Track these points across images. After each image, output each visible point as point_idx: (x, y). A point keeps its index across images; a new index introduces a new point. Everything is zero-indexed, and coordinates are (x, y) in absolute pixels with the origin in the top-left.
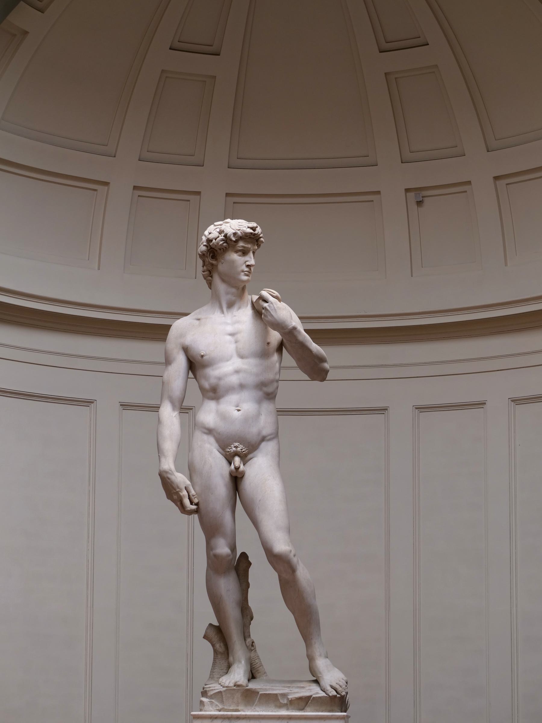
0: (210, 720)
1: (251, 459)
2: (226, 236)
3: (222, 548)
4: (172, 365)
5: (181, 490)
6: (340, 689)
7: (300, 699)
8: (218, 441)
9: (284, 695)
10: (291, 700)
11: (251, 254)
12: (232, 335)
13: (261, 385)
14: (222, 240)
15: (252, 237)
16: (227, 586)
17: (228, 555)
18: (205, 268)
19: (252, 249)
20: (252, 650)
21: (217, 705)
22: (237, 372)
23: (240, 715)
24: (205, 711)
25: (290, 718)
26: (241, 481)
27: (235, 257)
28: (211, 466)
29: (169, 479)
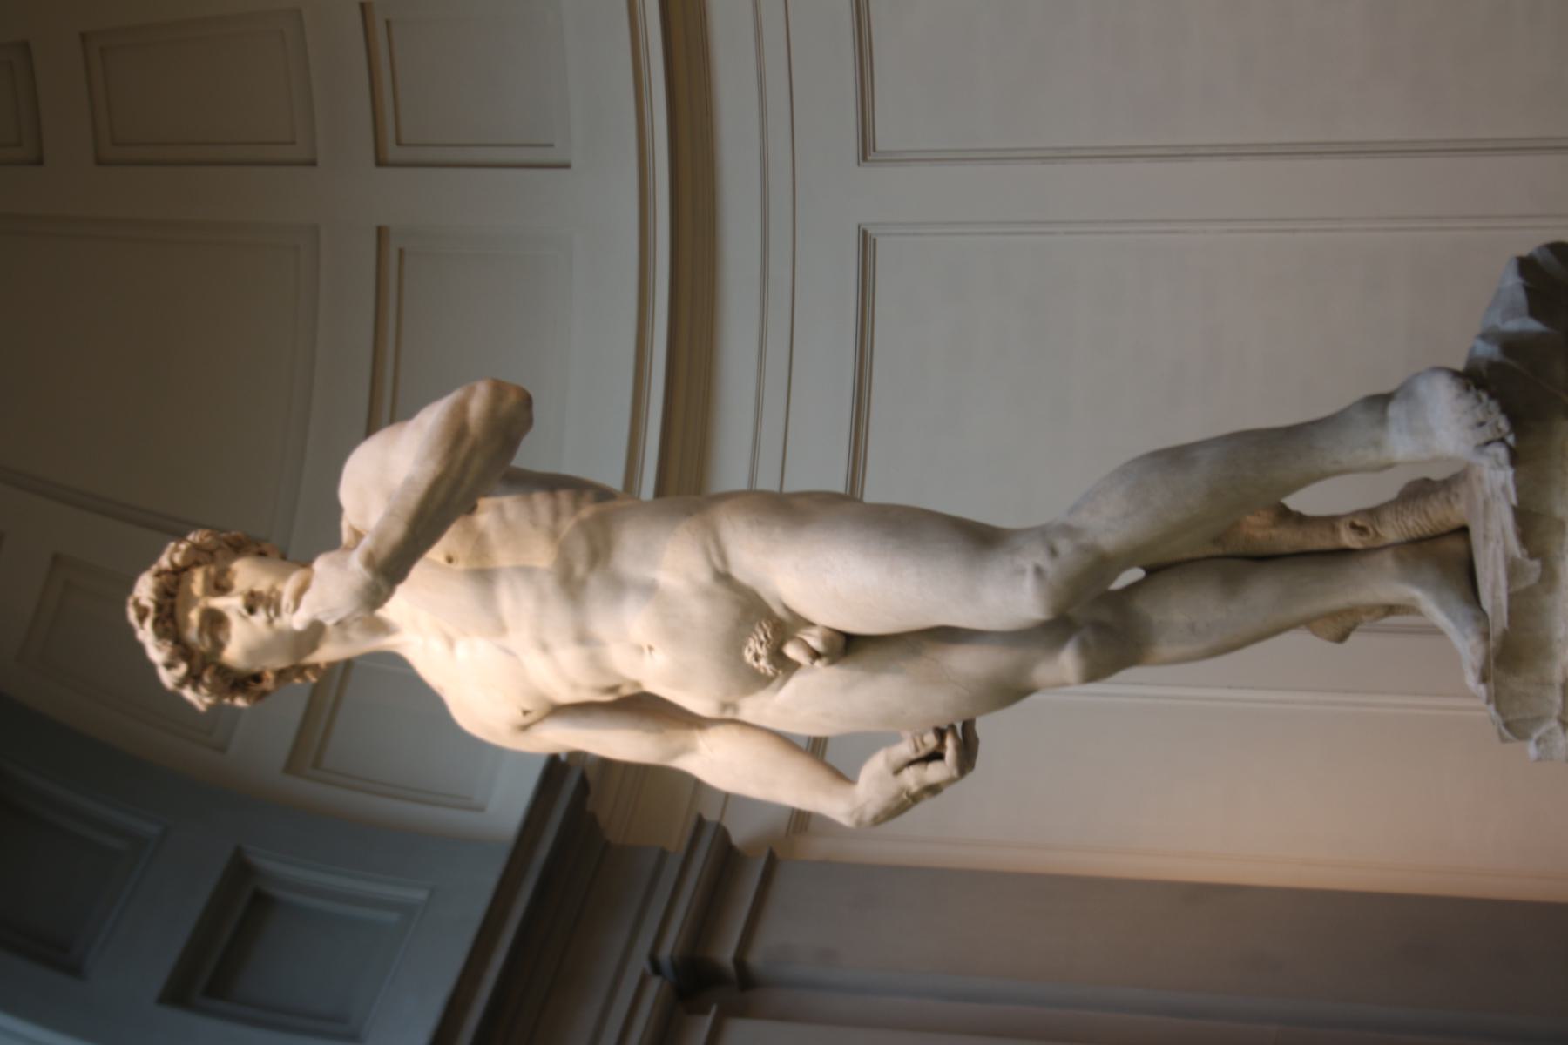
1: (787, 608)
2: (182, 683)
3: (1067, 661)
5: (903, 790)
6: (1487, 433)
7: (1524, 537)
9: (1513, 570)
13: (570, 586)
14: (195, 689)
16: (1180, 612)
17: (1084, 649)
19: (202, 604)
20: (1377, 534)
21: (1550, 732)
22: (545, 648)
27: (234, 652)
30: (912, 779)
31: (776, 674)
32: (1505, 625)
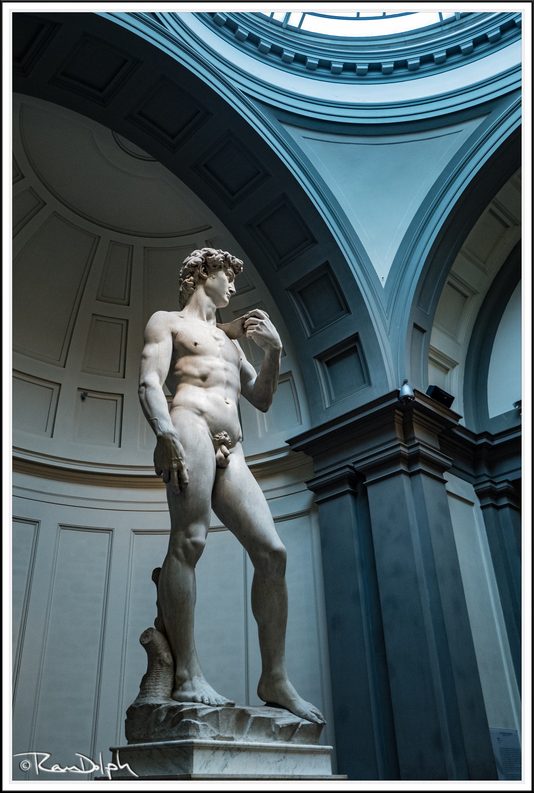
0: (211, 752)
4: (160, 343)
8: (209, 424)
10: (282, 727)
11: (232, 283)
12: (217, 339)
14: (222, 258)
15: (237, 271)
18: (192, 278)
22: (226, 369)
23: (243, 745)
24: (201, 738)
25: (286, 751)
26: (224, 472)
28: (206, 446)
29: (174, 442)
30: (183, 463)
31: (214, 437)
32: (253, 716)
